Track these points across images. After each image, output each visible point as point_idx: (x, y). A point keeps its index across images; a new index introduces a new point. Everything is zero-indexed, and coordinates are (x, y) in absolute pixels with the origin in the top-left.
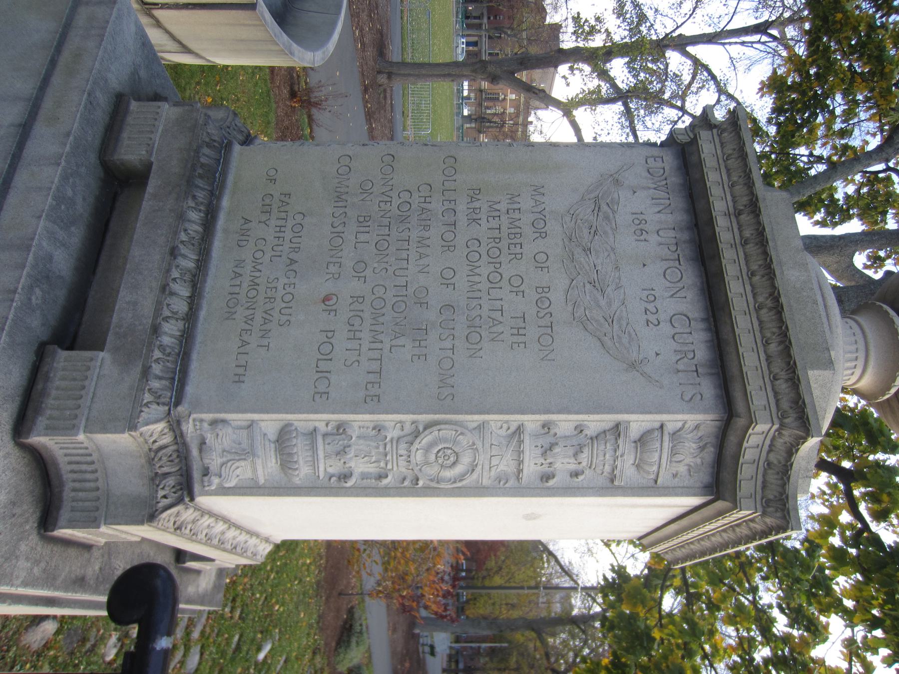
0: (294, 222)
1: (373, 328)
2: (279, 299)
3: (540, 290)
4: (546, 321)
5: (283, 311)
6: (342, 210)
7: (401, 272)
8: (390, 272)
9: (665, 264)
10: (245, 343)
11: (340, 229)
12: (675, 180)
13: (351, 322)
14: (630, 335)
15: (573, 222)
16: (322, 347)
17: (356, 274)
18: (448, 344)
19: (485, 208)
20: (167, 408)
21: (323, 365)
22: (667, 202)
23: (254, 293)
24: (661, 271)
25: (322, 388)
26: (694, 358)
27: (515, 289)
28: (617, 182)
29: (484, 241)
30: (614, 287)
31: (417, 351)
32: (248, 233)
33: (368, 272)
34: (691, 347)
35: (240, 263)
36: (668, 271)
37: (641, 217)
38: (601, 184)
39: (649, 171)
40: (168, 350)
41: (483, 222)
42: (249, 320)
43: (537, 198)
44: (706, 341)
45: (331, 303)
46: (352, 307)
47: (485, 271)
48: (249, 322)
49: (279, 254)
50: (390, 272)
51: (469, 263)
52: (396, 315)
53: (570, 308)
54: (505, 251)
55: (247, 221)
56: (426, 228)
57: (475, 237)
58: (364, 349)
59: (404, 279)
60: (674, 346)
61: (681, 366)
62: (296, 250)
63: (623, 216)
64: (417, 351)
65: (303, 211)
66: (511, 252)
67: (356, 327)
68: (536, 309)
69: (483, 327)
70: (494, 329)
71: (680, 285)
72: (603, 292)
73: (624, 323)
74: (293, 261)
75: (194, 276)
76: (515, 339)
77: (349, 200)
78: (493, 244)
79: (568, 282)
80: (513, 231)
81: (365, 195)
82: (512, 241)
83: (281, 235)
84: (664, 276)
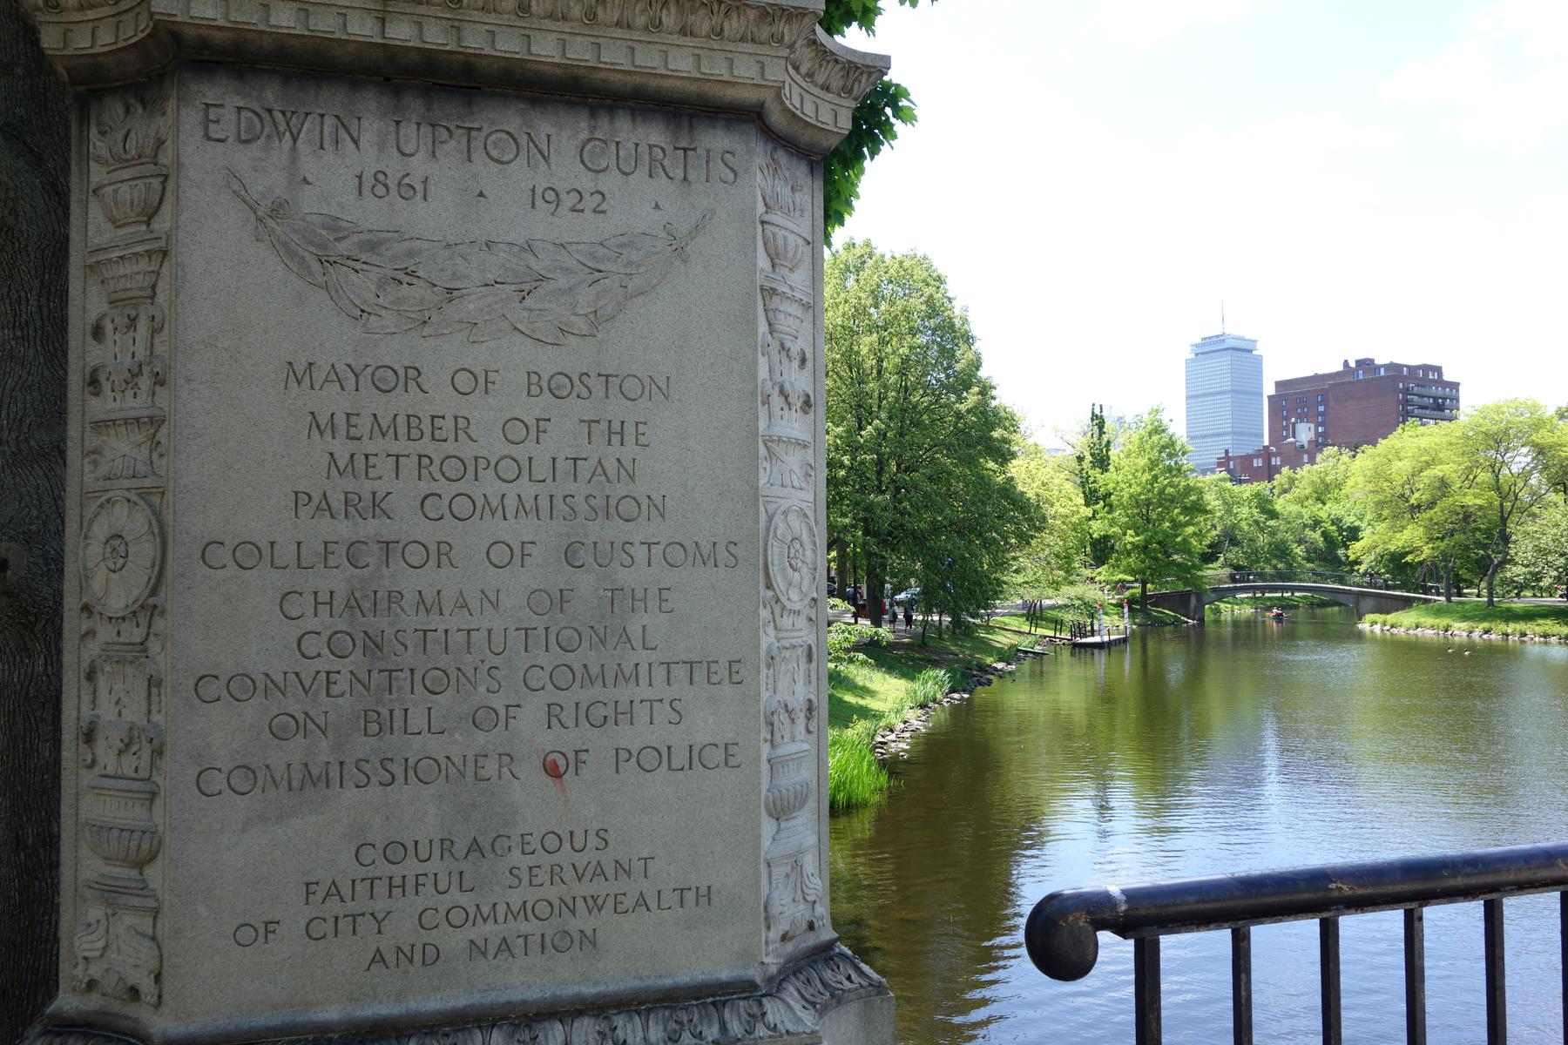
0: (381, 861)
1: (610, 682)
2: (554, 859)
3: (535, 390)
4: (597, 385)
5: (578, 846)
6: (350, 769)
7: (498, 640)
8: (497, 661)
9: (479, 156)
10: (642, 901)
11: (397, 769)
12: (271, 94)
13: (601, 720)
14: (621, 246)
15: (383, 313)
16: (647, 766)
17: (502, 723)
18: (640, 553)
19: (348, 484)
20: (764, 1000)
21: (680, 759)
22: (329, 122)
23: (541, 906)
24: (495, 167)
25: (719, 755)
26: (663, 150)
27: (533, 433)
28: (277, 211)
29: (425, 487)
30: (528, 256)
31: (653, 604)
32: (407, 949)
33: (498, 703)
34: (643, 149)
35: (476, 949)
36: (494, 153)
37: (368, 182)
38: (284, 244)
39: (246, 142)
40: (672, 1025)
41: (380, 488)
42: (594, 904)
43: (319, 377)
44: (634, 120)
45: (561, 762)
46: (570, 723)
47: (489, 486)
48: (600, 902)
49: (456, 877)
50: (497, 661)
51: (477, 517)
52: (585, 644)
53: (572, 340)
54: (449, 447)
55: (378, 958)
56: (395, 597)
57: (418, 503)
58: (650, 693)
59: (512, 634)
60: (641, 174)
61: (679, 173)
62: (447, 845)
63: (370, 214)
64: (653, 604)
65: (353, 849)
66: (452, 436)
67: (610, 712)
68: (573, 399)
69: (608, 492)
70: (612, 472)
71: (523, 140)
72: (543, 279)
73: (601, 251)
74: (475, 846)
75: (517, 1026)
76: (630, 438)
77: (323, 758)
78: (435, 468)
79: (518, 338)
80: (402, 430)
81: (311, 726)
82: (428, 434)
83: (410, 882)
84: (503, 163)
